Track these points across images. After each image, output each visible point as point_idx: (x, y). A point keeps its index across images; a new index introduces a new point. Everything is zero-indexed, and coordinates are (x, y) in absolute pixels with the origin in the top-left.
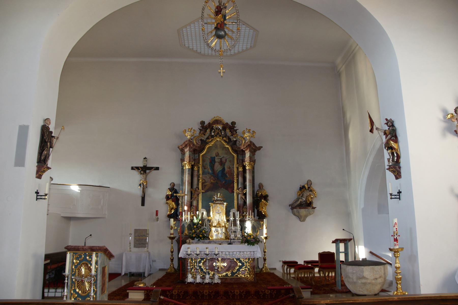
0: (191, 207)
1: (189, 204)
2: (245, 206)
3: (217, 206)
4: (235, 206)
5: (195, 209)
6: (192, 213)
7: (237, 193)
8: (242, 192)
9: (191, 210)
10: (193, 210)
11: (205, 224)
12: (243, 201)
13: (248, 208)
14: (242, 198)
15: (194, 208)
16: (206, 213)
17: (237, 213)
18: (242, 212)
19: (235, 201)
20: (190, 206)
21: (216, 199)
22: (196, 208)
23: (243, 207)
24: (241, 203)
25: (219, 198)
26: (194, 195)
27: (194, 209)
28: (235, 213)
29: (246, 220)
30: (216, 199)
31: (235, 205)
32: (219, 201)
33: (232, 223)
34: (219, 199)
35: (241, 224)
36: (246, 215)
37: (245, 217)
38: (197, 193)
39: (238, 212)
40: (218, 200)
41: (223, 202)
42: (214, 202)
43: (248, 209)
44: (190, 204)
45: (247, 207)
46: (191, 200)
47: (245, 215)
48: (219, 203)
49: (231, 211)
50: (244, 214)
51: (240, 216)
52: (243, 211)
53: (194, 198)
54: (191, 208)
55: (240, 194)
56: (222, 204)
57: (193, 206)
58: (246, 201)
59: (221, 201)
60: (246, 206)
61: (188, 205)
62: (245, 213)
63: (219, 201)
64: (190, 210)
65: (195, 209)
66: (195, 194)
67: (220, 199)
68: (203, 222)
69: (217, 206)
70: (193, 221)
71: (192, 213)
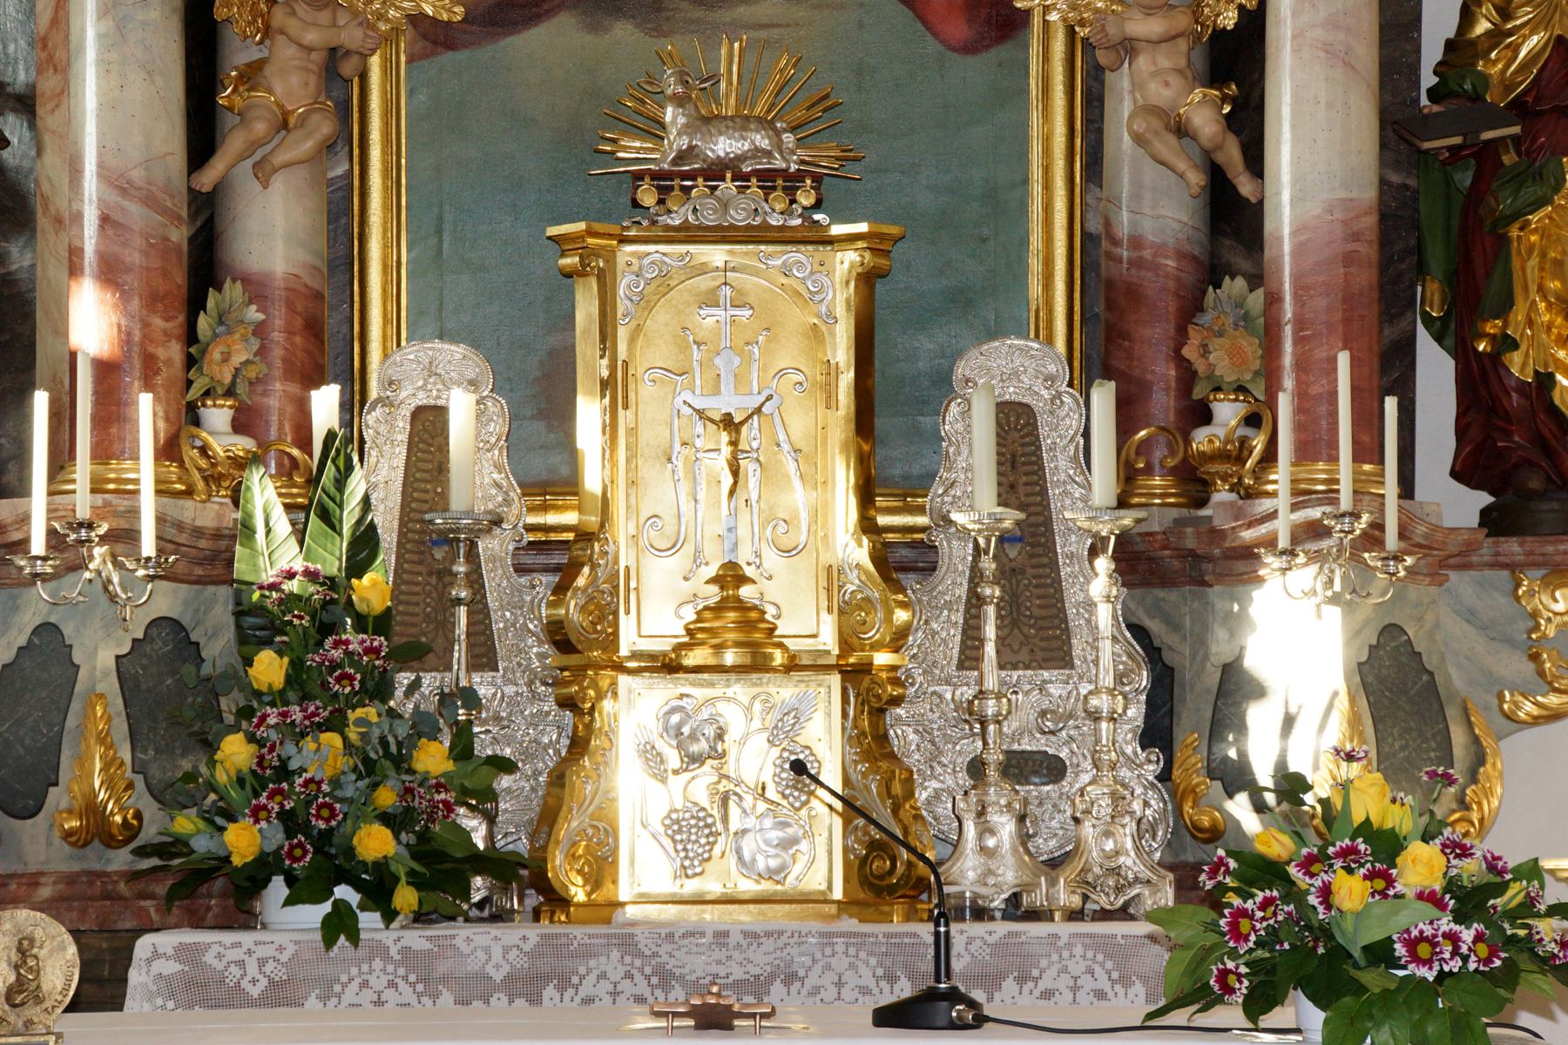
0: (195, 304)
1: (162, 247)
2: (1235, 286)
3: (703, 283)
4: (1035, 289)
5: (277, 336)
6: (218, 416)
7: (1071, 33)
8: (1183, 21)
9: (191, 362)
10: (238, 359)
11: (462, 612)
12: (1197, 179)
13: (1300, 323)
14: (1181, 130)
15: (253, 314)
16: (498, 427)
17: (1074, 423)
18: (1163, 403)
19: (1037, 189)
20: (180, 277)
21: (677, 141)
22: (314, 328)
23: (1191, 308)
24: (1150, 230)
25: (741, 122)
26: (252, 75)
27: (262, 352)
28: (1043, 421)
29: (1248, 535)
30: (681, 157)
31: (1035, 265)
32: (728, 187)
33: (975, 602)
34: (724, 146)
35: (1154, 626)
36: (1244, 445)
37: (1222, 495)
38: (311, 37)
39: (1103, 397)
40: (715, 171)
41: (806, 199)
42: (648, 197)
43: (1288, 331)
44: (179, 235)
45: (1273, 300)
46: (207, 179)
47: (1222, 456)
48: (739, 216)
49: (961, 369)
50: (1202, 439)
51: (1129, 475)
52: (1188, 376)
53: (260, 128)
54: (203, 323)
55: (1128, 48)
56: (783, 237)
57: (233, 291)
58: (1245, 187)
59: (767, 178)
60: (1256, 280)
61: (134, 257)
62: (1228, 413)
63: (728, 187)
64: (173, 352)
65: (277, 336)
66: (285, 52)
67: (757, 152)
68: (445, 575)
69: (703, 283)
70: (230, 562)
71: (218, 416)
